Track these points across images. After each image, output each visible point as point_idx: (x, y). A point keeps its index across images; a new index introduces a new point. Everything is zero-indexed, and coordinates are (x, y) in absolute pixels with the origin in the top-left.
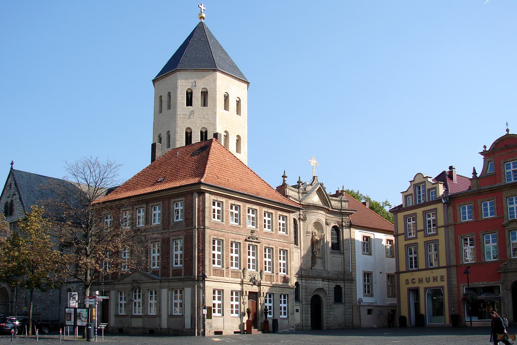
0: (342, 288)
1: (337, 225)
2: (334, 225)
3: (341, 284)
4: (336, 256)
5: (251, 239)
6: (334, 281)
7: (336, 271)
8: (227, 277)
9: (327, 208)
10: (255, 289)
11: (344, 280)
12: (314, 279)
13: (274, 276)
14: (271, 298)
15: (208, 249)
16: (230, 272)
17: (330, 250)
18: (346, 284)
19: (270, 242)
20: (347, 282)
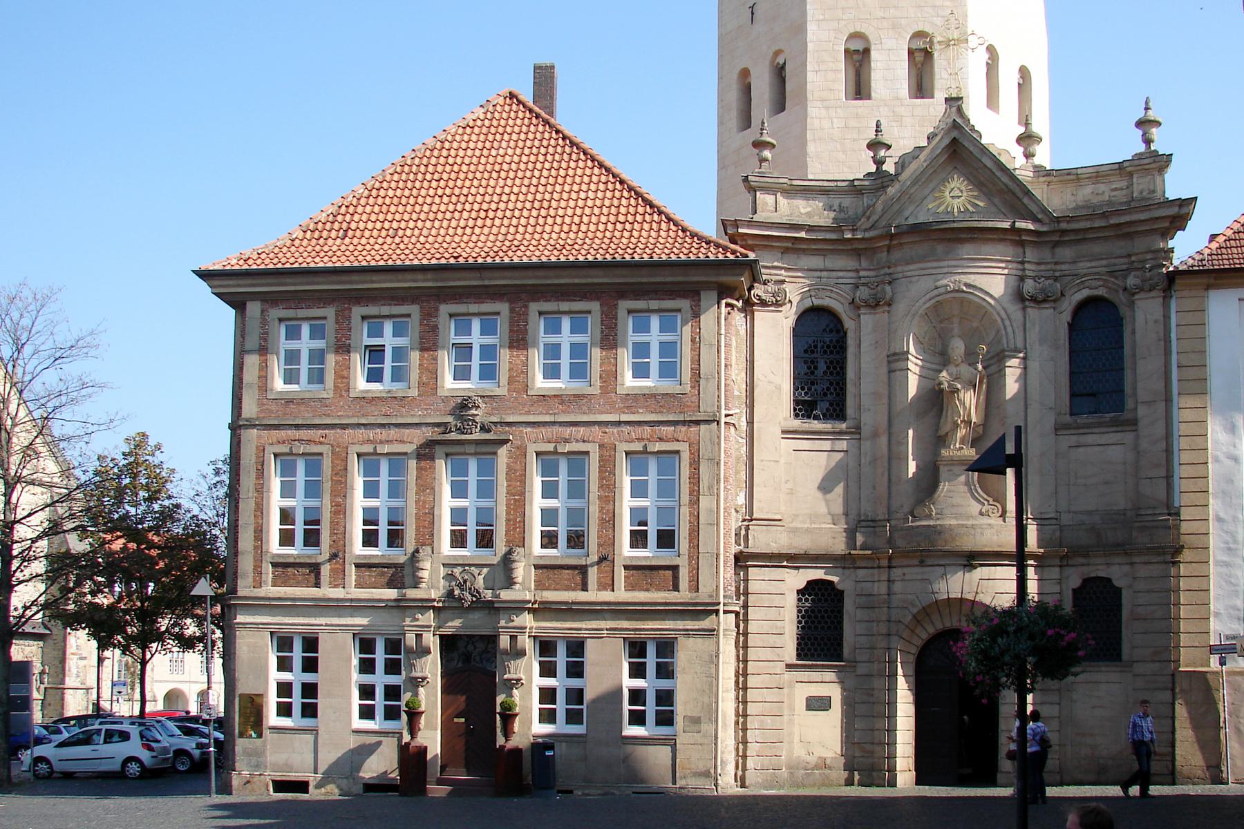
0: (1120, 590)
1: (1101, 292)
2: (1085, 293)
3: (1117, 572)
4: (1090, 439)
5: (454, 436)
6: (1070, 562)
7: (1090, 513)
8: (336, 586)
9: (1006, 225)
10: (477, 624)
11: (1123, 549)
12: (916, 562)
13: (675, 569)
14: (401, 654)
15: (251, 495)
16: (352, 572)
17: (1059, 414)
18: (1143, 571)
19: (567, 431)
20: (1146, 558)
